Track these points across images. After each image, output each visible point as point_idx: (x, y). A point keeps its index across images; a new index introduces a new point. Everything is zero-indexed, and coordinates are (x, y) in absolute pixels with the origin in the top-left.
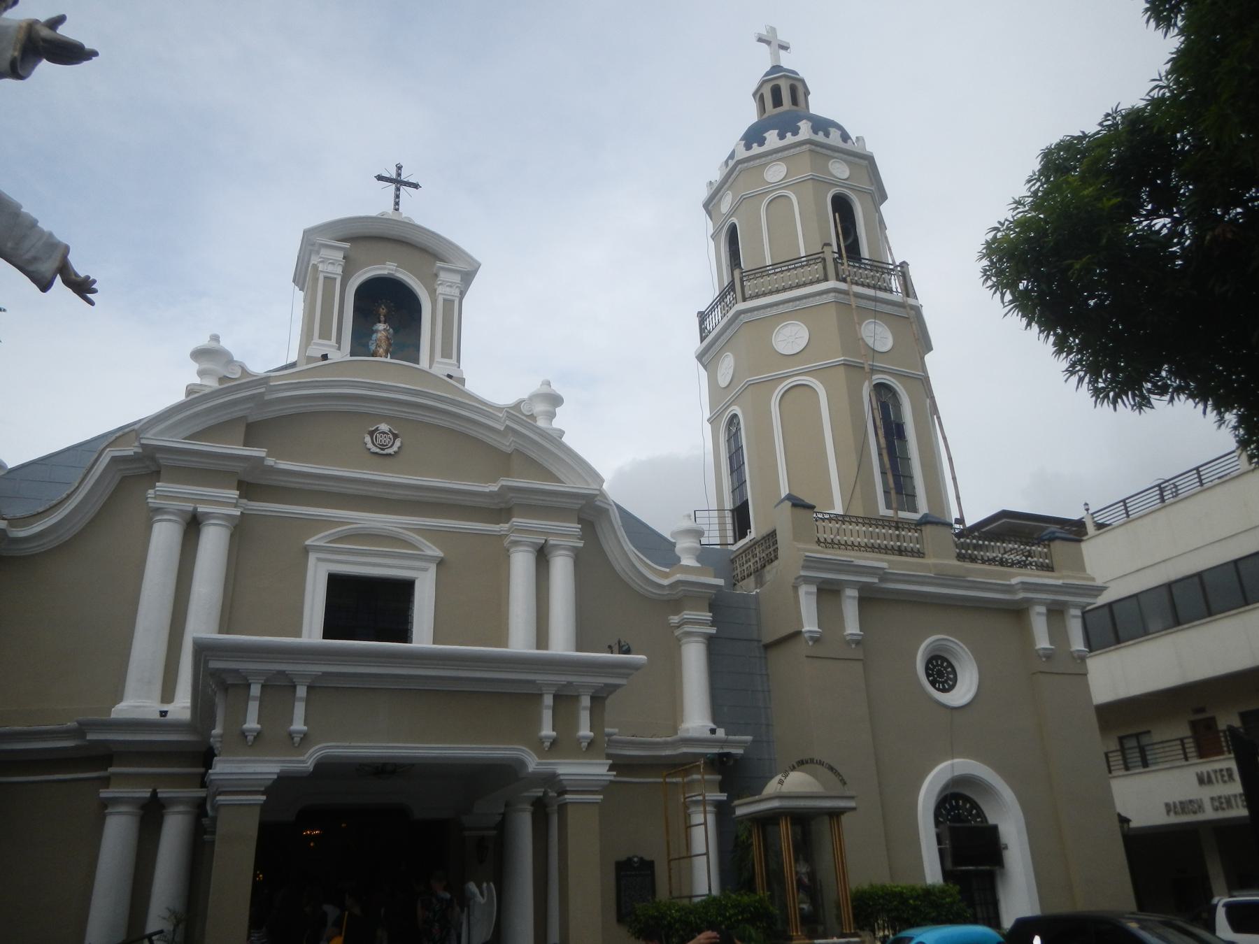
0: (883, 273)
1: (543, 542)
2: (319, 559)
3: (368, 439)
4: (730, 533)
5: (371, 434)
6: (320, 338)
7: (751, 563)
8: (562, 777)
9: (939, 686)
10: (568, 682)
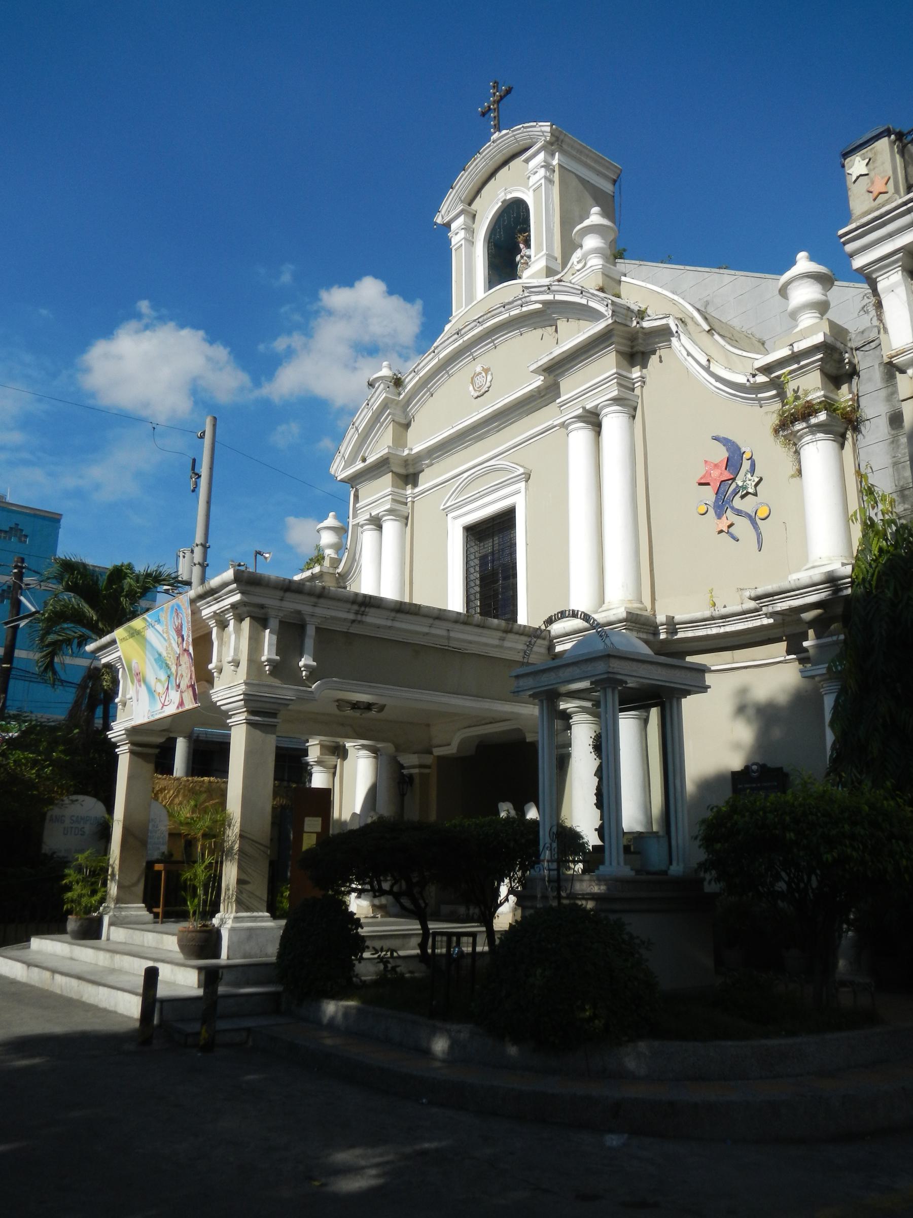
2: (455, 518)
3: (471, 388)
8: (219, 704)
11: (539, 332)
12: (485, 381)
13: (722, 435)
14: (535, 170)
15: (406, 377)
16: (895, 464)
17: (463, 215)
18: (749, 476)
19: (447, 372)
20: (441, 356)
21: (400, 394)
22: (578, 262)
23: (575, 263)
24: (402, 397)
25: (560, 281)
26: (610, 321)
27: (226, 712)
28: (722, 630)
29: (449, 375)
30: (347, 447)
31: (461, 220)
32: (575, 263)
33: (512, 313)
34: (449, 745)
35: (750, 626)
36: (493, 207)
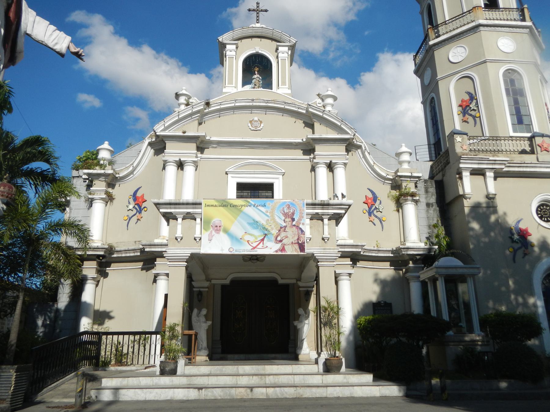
0: (509, 11)
1: (329, 161)
2: (232, 177)
3: (250, 125)
4: (434, 155)
5: (251, 122)
6: (228, 84)
7: (439, 167)
8: (315, 255)
9: (544, 219)
10: (316, 213)
11: (294, 119)
12: (259, 126)
13: (371, 189)
14: (283, 52)
15: (213, 104)
16: (428, 218)
17: (235, 46)
18: (380, 205)
19: (234, 112)
20: (236, 104)
21: (205, 109)
22: (319, 103)
23: (317, 103)
24: (206, 111)
25: (329, 111)
26: (352, 137)
27: (318, 259)
28: (377, 255)
29: (234, 113)
30: (169, 121)
31: (234, 47)
32: (317, 103)
33: (286, 107)
34: (226, 279)
35: (386, 256)
36: (250, 51)
